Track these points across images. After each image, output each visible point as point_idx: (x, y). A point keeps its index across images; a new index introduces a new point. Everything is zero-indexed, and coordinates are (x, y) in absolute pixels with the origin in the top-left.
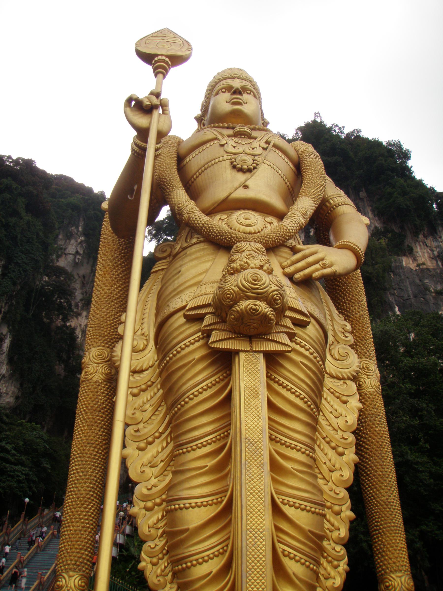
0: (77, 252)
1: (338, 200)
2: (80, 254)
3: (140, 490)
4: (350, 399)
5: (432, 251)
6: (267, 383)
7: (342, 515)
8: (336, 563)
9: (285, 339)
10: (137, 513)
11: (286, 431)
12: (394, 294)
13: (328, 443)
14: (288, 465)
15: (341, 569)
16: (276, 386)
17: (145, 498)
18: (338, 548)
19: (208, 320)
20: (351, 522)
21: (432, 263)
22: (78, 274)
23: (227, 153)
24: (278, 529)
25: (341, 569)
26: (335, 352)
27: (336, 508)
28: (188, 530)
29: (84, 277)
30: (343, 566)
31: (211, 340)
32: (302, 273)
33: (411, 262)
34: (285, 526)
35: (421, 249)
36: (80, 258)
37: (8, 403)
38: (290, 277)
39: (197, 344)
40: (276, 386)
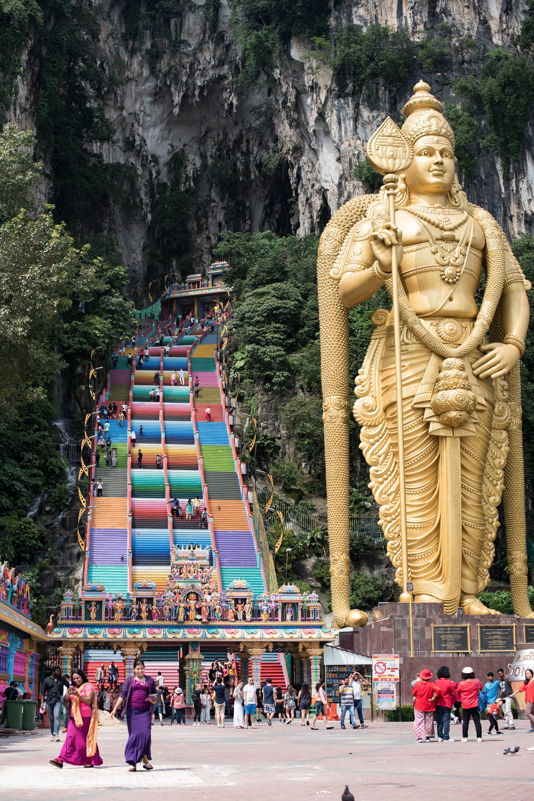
3: (382, 509)
4: (504, 445)
6: (461, 453)
7: (494, 524)
8: (488, 552)
9: (472, 428)
10: (383, 524)
11: (468, 481)
13: (488, 478)
14: (469, 502)
15: (491, 556)
16: (465, 454)
17: (386, 515)
18: (490, 544)
19: (428, 413)
20: (499, 529)
23: (438, 263)
25: (491, 556)
27: (490, 520)
28: (416, 540)
30: (492, 554)
31: (430, 430)
32: (485, 373)
38: (477, 376)
39: (420, 427)
40: (465, 454)
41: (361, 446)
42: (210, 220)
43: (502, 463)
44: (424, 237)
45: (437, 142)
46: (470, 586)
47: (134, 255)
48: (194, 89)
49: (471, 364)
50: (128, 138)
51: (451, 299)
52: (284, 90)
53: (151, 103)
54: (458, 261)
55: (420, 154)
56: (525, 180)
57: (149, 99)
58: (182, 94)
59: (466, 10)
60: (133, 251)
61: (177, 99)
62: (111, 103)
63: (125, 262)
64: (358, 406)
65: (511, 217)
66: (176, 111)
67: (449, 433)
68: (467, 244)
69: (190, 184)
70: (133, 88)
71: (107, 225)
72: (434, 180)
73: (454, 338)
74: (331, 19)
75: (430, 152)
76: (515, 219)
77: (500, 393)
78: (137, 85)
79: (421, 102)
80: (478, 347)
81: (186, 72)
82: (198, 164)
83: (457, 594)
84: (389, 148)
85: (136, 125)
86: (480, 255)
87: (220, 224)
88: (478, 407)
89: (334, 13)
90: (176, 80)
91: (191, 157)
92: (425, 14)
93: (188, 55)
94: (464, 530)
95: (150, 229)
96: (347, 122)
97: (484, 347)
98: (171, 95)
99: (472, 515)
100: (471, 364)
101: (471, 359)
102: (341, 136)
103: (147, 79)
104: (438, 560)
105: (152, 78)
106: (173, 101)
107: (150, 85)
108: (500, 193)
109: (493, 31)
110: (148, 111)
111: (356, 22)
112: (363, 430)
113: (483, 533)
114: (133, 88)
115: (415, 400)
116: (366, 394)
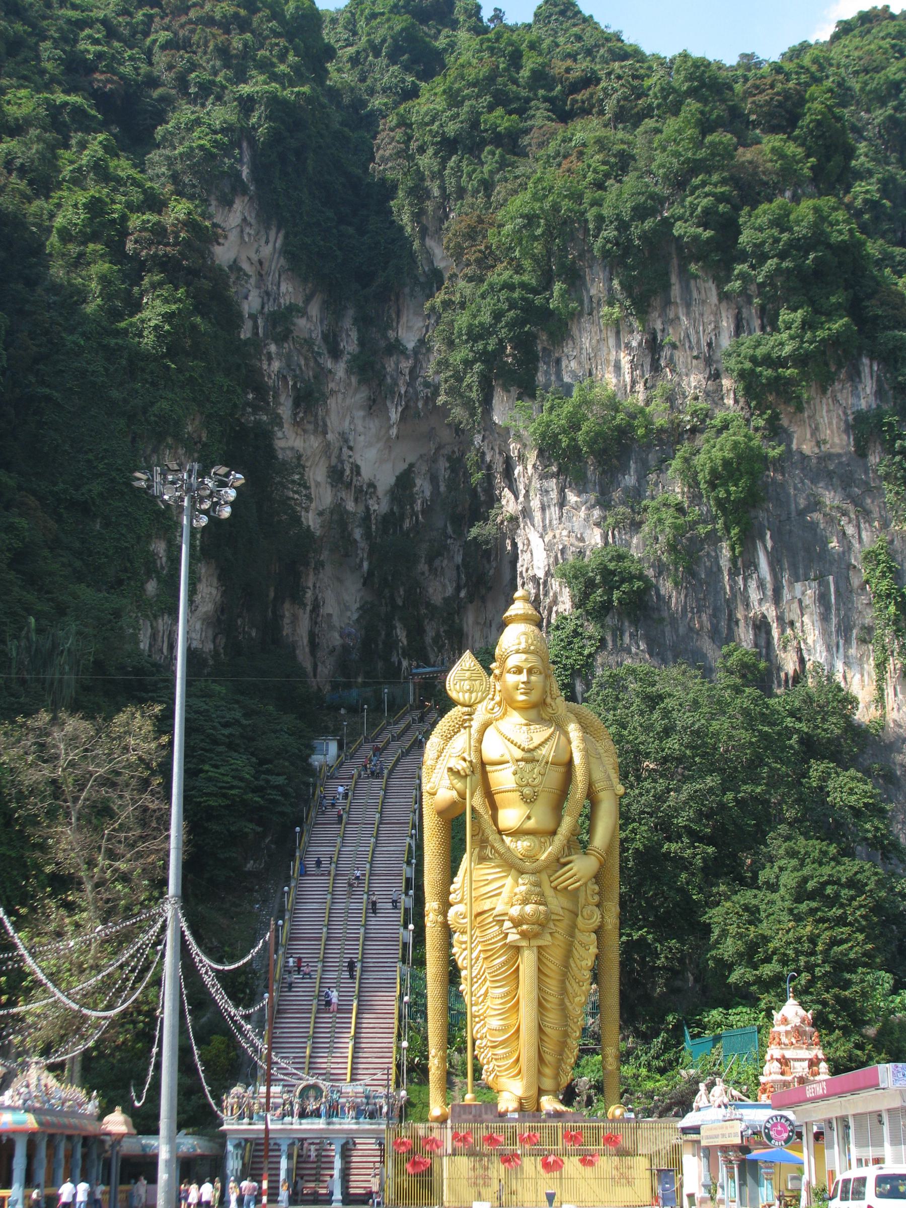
0: (244, 219)
1: (599, 786)
2: (251, 225)
5: (845, 414)
9: (549, 937)
12: (767, 510)
14: (548, 1006)
17: (476, 1017)
19: (508, 924)
21: (841, 440)
22: (249, 259)
24: (541, 1040)
26: (585, 913)
29: (261, 263)
33: (808, 436)
34: (545, 1038)
35: (828, 411)
36: (252, 232)
37: (206, 613)
38: (555, 888)
41: (454, 951)
42: (446, 562)
43: (590, 964)
44: (507, 757)
45: (526, 660)
46: (548, 1084)
47: (349, 614)
48: (417, 400)
49: (550, 876)
50: (335, 467)
51: (529, 818)
52: (488, 458)
53: (364, 418)
54: (536, 782)
55: (509, 672)
56: (755, 576)
57: (361, 413)
58: (400, 409)
59: (695, 362)
60: (347, 608)
61: (394, 416)
62: (310, 427)
63: (337, 624)
64: (452, 912)
65: (737, 622)
66: (394, 431)
67: (524, 943)
68: (547, 763)
69: (417, 518)
70: (340, 401)
71: (311, 585)
72: (523, 698)
73: (532, 854)
74: (539, 374)
75: (519, 671)
76: (742, 623)
77: (590, 898)
78: (344, 399)
79: (516, 615)
80: (558, 860)
81: (405, 380)
82: (428, 494)
83: (534, 1091)
84: (467, 682)
85: (345, 450)
86: (562, 769)
87: (458, 567)
88: (554, 917)
89: (542, 367)
90: (392, 391)
91: (418, 482)
92: (647, 367)
93: (407, 358)
94: (541, 1030)
95: (367, 581)
96: (552, 508)
97: (563, 860)
98: (387, 410)
99: (553, 1017)
100: (550, 876)
101: (550, 872)
102: (544, 526)
103: (356, 391)
104: (518, 1060)
105: (364, 388)
106: (389, 418)
107: (362, 395)
108: (725, 593)
109: (724, 391)
110: (360, 428)
111: (567, 379)
112: (456, 936)
113: (566, 1034)
114: (340, 401)
115: (495, 912)
116: (460, 902)
